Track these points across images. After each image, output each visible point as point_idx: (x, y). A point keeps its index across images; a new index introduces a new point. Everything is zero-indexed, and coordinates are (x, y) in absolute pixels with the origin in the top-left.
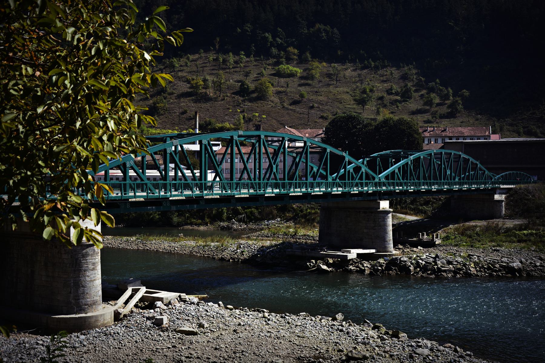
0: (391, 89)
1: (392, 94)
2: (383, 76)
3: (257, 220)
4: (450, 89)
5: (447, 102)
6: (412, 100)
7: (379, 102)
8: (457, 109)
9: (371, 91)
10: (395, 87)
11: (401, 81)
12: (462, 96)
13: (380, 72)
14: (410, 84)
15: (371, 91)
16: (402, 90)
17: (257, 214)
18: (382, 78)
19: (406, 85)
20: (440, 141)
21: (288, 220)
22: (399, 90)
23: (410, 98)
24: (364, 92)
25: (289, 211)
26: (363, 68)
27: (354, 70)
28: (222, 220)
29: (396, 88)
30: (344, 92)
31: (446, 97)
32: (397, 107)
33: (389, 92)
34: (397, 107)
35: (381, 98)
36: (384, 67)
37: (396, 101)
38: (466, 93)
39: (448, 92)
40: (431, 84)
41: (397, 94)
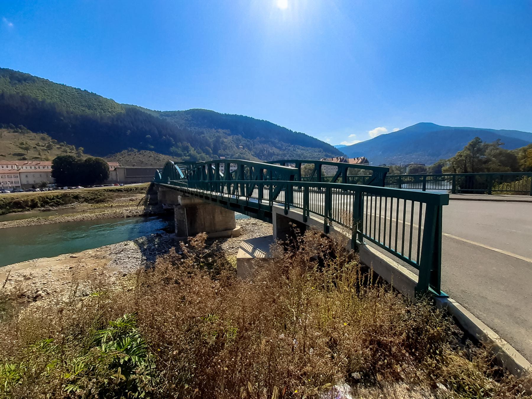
0: (38, 144)
1: (40, 146)
3: (62, 204)
4: (74, 146)
6: (53, 150)
9: (26, 144)
11: (42, 140)
15: (26, 144)
17: (61, 202)
18: (29, 138)
20: (113, 167)
24: (22, 144)
25: (80, 198)
26: (15, 132)
27: (9, 132)
28: (38, 207)
29: (41, 144)
30: (8, 143)
31: (72, 149)
32: (48, 152)
33: (38, 145)
34: (48, 152)
35: (35, 148)
37: (46, 150)
38: (83, 149)
39: (73, 147)
40: (62, 143)
41: (43, 146)
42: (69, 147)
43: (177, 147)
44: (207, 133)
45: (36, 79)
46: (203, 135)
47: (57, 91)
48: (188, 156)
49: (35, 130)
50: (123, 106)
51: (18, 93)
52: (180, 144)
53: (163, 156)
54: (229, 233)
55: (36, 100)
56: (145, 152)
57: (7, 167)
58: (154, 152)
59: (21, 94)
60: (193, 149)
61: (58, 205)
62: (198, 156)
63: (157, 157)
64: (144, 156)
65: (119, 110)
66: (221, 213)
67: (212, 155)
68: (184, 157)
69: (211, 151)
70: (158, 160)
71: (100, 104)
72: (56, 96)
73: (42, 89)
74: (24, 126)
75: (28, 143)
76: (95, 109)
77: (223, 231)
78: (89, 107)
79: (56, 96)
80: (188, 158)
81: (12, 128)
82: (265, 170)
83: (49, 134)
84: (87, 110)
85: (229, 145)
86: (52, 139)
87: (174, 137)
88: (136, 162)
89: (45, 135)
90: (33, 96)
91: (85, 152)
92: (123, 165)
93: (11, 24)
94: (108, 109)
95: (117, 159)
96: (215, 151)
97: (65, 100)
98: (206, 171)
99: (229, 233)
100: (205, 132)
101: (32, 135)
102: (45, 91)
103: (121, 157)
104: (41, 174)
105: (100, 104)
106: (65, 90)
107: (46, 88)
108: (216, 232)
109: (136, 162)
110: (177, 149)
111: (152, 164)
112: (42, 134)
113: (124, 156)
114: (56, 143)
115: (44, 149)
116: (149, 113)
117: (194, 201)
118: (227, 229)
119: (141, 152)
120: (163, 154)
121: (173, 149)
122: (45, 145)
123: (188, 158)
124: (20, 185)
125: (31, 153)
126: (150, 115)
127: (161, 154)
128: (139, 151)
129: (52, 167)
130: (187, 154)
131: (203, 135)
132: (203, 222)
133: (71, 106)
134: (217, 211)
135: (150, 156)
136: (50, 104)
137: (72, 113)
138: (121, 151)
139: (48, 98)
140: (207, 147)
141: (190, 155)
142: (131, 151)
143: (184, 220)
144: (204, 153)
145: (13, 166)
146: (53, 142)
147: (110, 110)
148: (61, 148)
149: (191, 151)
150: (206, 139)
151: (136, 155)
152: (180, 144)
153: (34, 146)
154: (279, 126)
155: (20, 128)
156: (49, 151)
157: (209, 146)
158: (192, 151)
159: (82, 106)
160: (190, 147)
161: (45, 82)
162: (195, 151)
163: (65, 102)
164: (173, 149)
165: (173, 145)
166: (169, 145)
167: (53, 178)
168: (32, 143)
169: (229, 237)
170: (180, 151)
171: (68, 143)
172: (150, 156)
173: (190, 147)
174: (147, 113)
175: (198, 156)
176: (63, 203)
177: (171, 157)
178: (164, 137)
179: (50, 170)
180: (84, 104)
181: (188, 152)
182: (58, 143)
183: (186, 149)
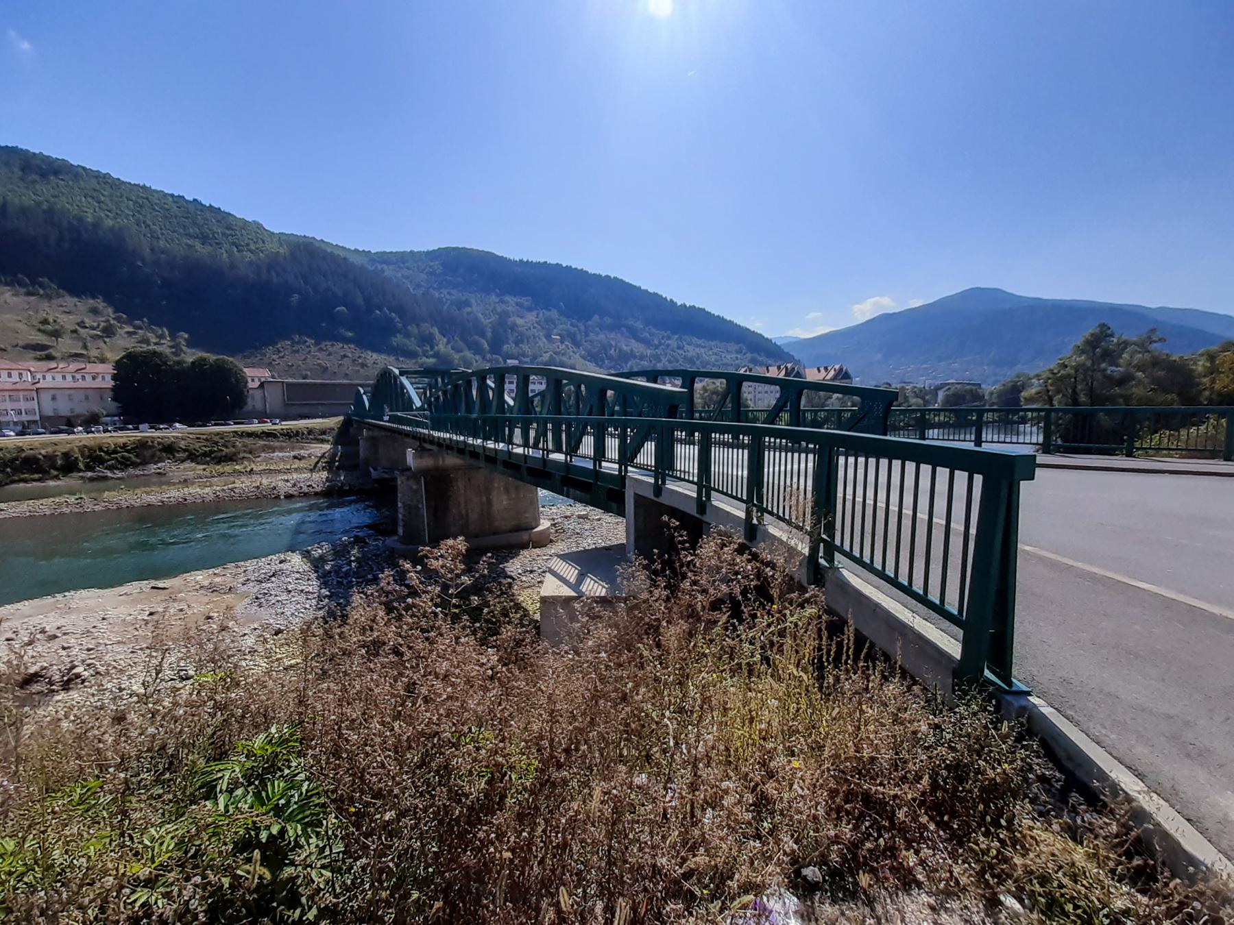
0: (83, 322)
1: (86, 327)
2: (62, 306)
3: (135, 465)
4: (165, 330)
5: (162, 342)
7: (75, 335)
8: (182, 350)
9: (55, 321)
10: (86, 320)
12: (182, 337)
13: (54, 302)
14: (112, 322)
15: (55, 321)
16: (99, 325)
17: (134, 459)
19: (108, 321)
20: (256, 380)
21: (183, 461)
22: (95, 324)
23: (114, 334)
24: (45, 322)
26: (29, 294)
28: (80, 470)
29: (88, 322)
31: (162, 337)
33: (82, 324)
34: (105, 343)
35: (75, 331)
36: (59, 296)
38: (186, 336)
40: (138, 322)
41: (93, 328)
42: (153, 332)
43: (407, 335)
44: (478, 305)
45: (80, 170)
46: (469, 309)
47: (129, 199)
48: (434, 356)
49: (76, 292)
50: (283, 238)
51: (38, 204)
52: (412, 329)
53: (375, 356)
54: (525, 536)
55: (80, 220)
56: (332, 345)
57: (10, 375)
58: (352, 346)
59: (45, 206)
60: (445, 340)
61: (127, 466)
62: (457, 356)
63: (360, 357)
64: (330, 354)
65: (272, 247)
66: (507, 491)
67: (488, 356)
68: (424, 359)
69: (486, 346)
70: (363, 365)
71: (228, 232)
72: (126, 211)
73: (95, 194)
74: (51, 280)
75: (59, 320)
76: (217, 244)
77: (511, 531)
78: (204, 239)
79: (126, 211)
80: (432, 360)
81: (21, 284)
82: (610, 393)
83: (109, 300)
84: (198, 245)
85: (530, 333)
86: (115, 312)
87: (400, 310)
88: (310, 370)
89: (100, 304)
90: (74, 210)
91: (190, 344)
92: (280, 376)
93: (26, 46)
94: (248, 245)
95: (268, 361)
96: (496, 346)
97: (148, 222)
98: (474, 393)
99: (525, 536)
100: (473, 301)
101: (70, 301)
102: (103, 199)
103: (274, 357)
104: (90, 392)
105: (228, 232)
106: (147, 199)
107: (105, 193)
108: (495, 533)
109: (310, 370)
110: (407, 341)
111: (346, 375)
112: (91, 301)
113: (281, 355)
114: (123, 323)
115: (97, 335)
116: (342, 254)
117: (443, 461)
118: (518, 529)
119: (323, 346)
120: (373, 351)
121: (397, 340)
122: (99, 325)
123: (432, 360)
124: (38, 418)
125: (66, 344)
126: (345, 259)
127: (369, 353)
128: (317, 344)
129: (114, 378)
130: (431, 353)
131: (469, 309)
132: (463, 512)
133: (162, 234)
134: (496, 485)
135: (345, 356)
136: (112, 229)
137: (162, 253)
138: (277, 344)
139: (107, 216)
140: (476, 337)
141: (436, 355)
142: (298, 343)
143: (420, 506)
144: (469, 349)
145: (24, 373)
146: (118, 319)
147: (252, 247)
148: (135, 333)
149: (441, 346)
150: (476, 319)
151: (310, 352)
152: (412, 329)
153: (73, 328)
154: (647, 291)
155: (42, 286)
156: (107, 340)
157: (483, 335)
158: (442, 346)
159: (189, 236)
160: (437, 335)
161: (103, 179)
162: (449, 346)
163: (147, 226)
164: (397, 340)
165: (399, 331)
166: (388, 329)
167: (116, 404)
168: (68, 322)
169: (525, 546)
170: (411, 344)
171: (152, 322)
172: (345, 356)
173: (437, 335)
174: (339, 255)
175: (457, 356)
176: (138, 461)
177: (392, 358)
178: (378, 312)
179: (110, 383)
180: (191, 231)
181: (432, 348)
182: (130, 322)
183: (428, 340)
